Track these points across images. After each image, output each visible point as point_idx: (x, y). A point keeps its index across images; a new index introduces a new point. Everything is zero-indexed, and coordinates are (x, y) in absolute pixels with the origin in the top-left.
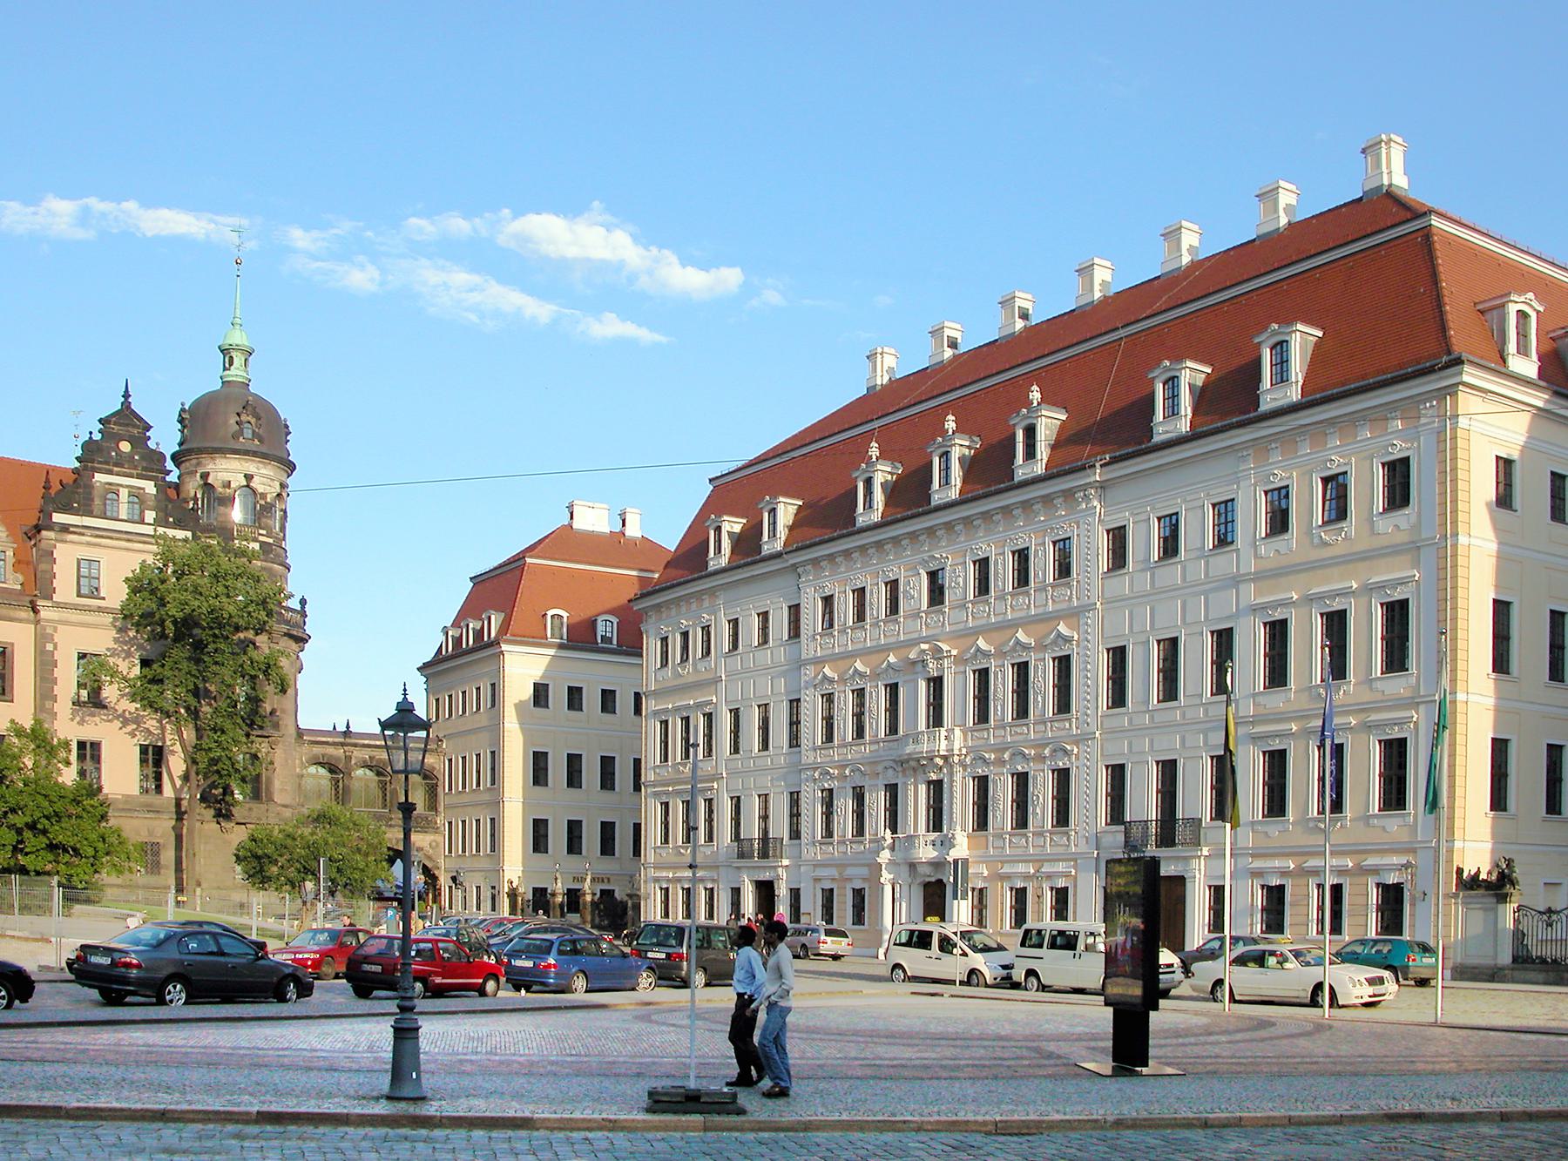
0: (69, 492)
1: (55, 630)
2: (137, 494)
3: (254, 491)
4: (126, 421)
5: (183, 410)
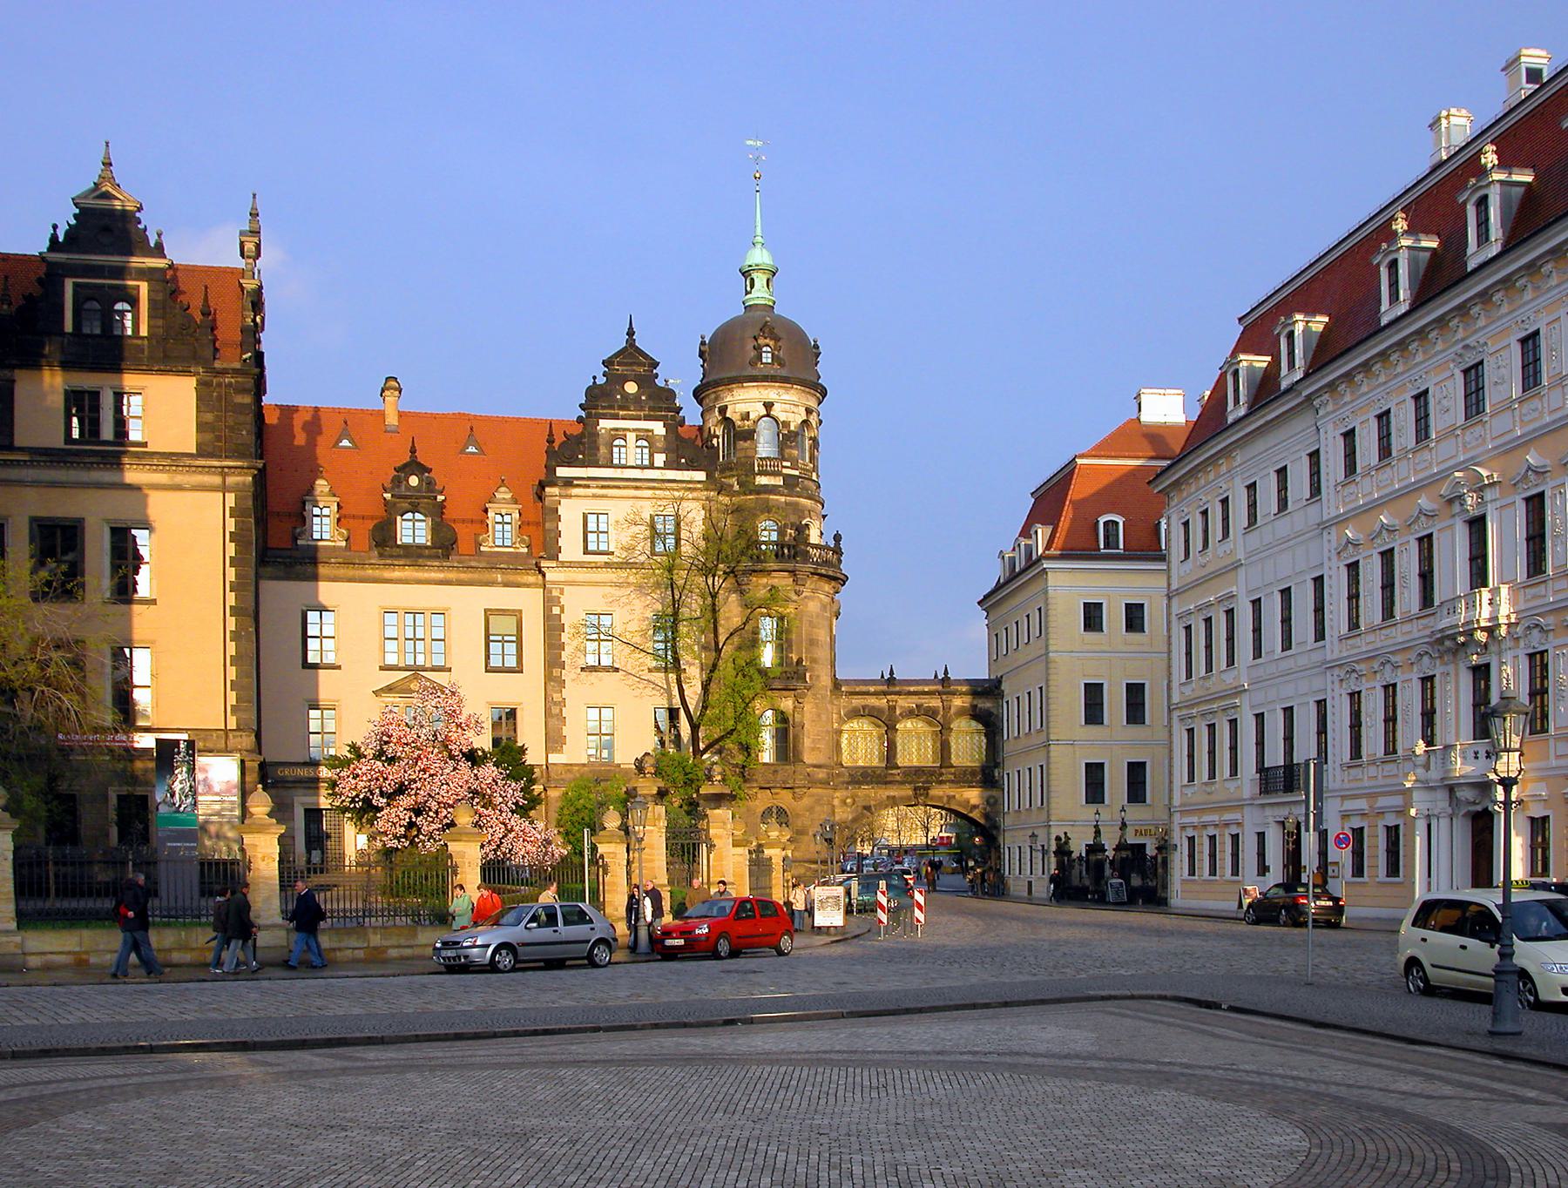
0: (577, 445)
2: (645, 435)
4: (630, 360)
5: (703, 343)
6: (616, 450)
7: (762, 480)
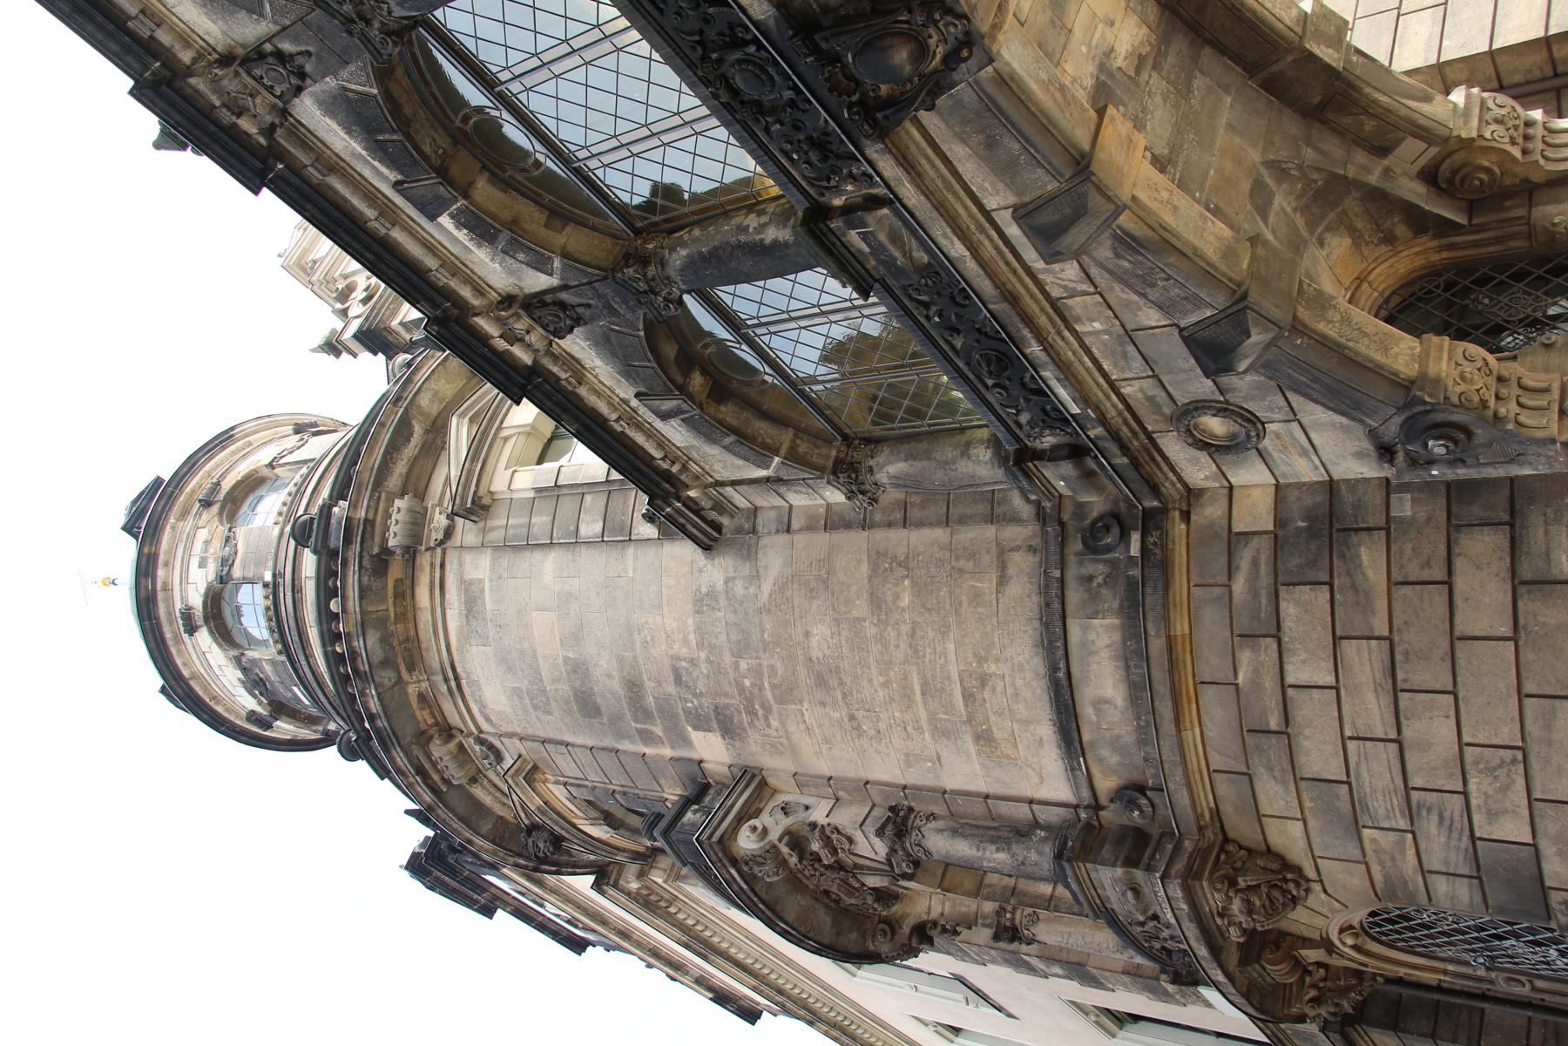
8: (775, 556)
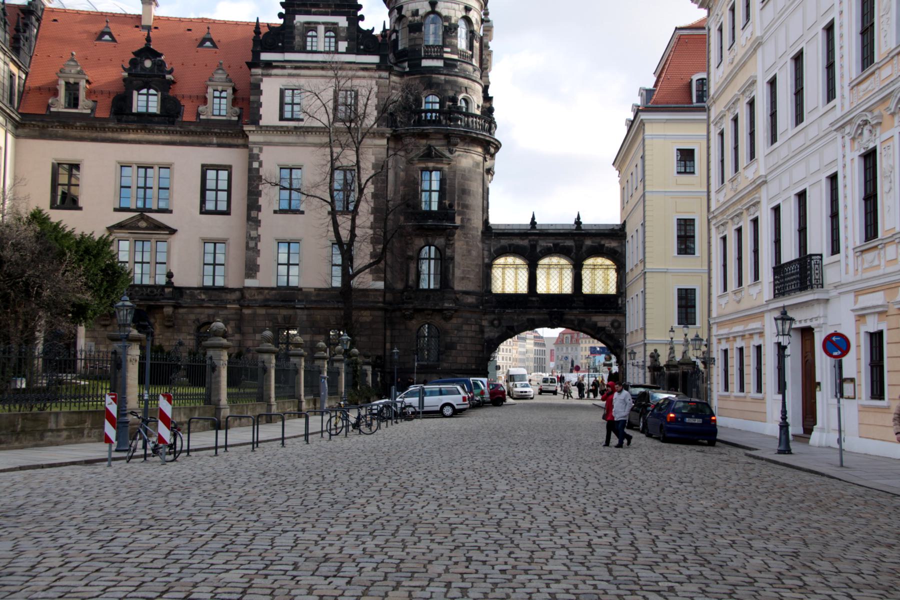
1: (261, 150)
2: (331, 28)
3: (439, 14)
6: (309, 39)
7: (426, 63)
8: (480, 245)
